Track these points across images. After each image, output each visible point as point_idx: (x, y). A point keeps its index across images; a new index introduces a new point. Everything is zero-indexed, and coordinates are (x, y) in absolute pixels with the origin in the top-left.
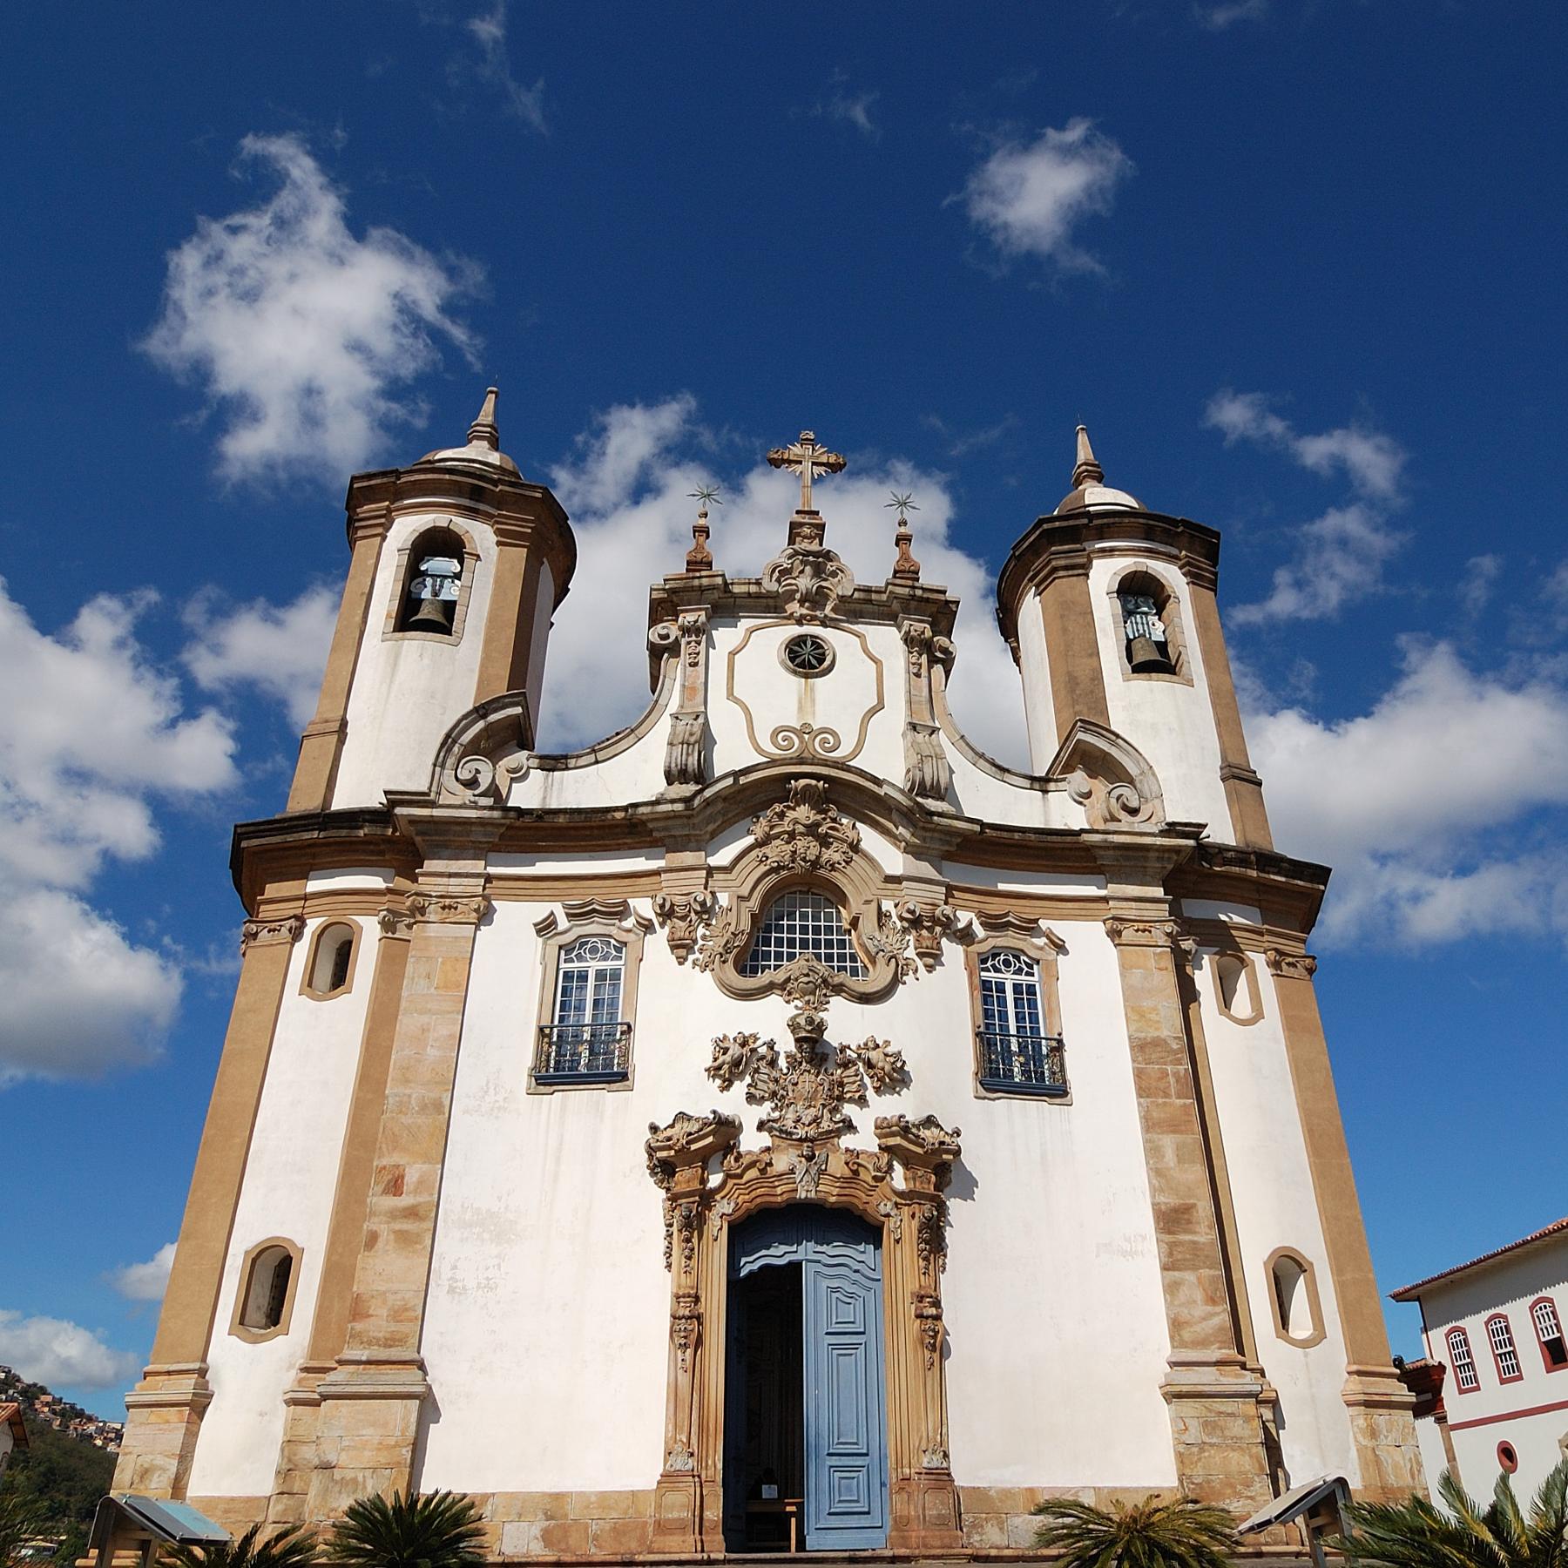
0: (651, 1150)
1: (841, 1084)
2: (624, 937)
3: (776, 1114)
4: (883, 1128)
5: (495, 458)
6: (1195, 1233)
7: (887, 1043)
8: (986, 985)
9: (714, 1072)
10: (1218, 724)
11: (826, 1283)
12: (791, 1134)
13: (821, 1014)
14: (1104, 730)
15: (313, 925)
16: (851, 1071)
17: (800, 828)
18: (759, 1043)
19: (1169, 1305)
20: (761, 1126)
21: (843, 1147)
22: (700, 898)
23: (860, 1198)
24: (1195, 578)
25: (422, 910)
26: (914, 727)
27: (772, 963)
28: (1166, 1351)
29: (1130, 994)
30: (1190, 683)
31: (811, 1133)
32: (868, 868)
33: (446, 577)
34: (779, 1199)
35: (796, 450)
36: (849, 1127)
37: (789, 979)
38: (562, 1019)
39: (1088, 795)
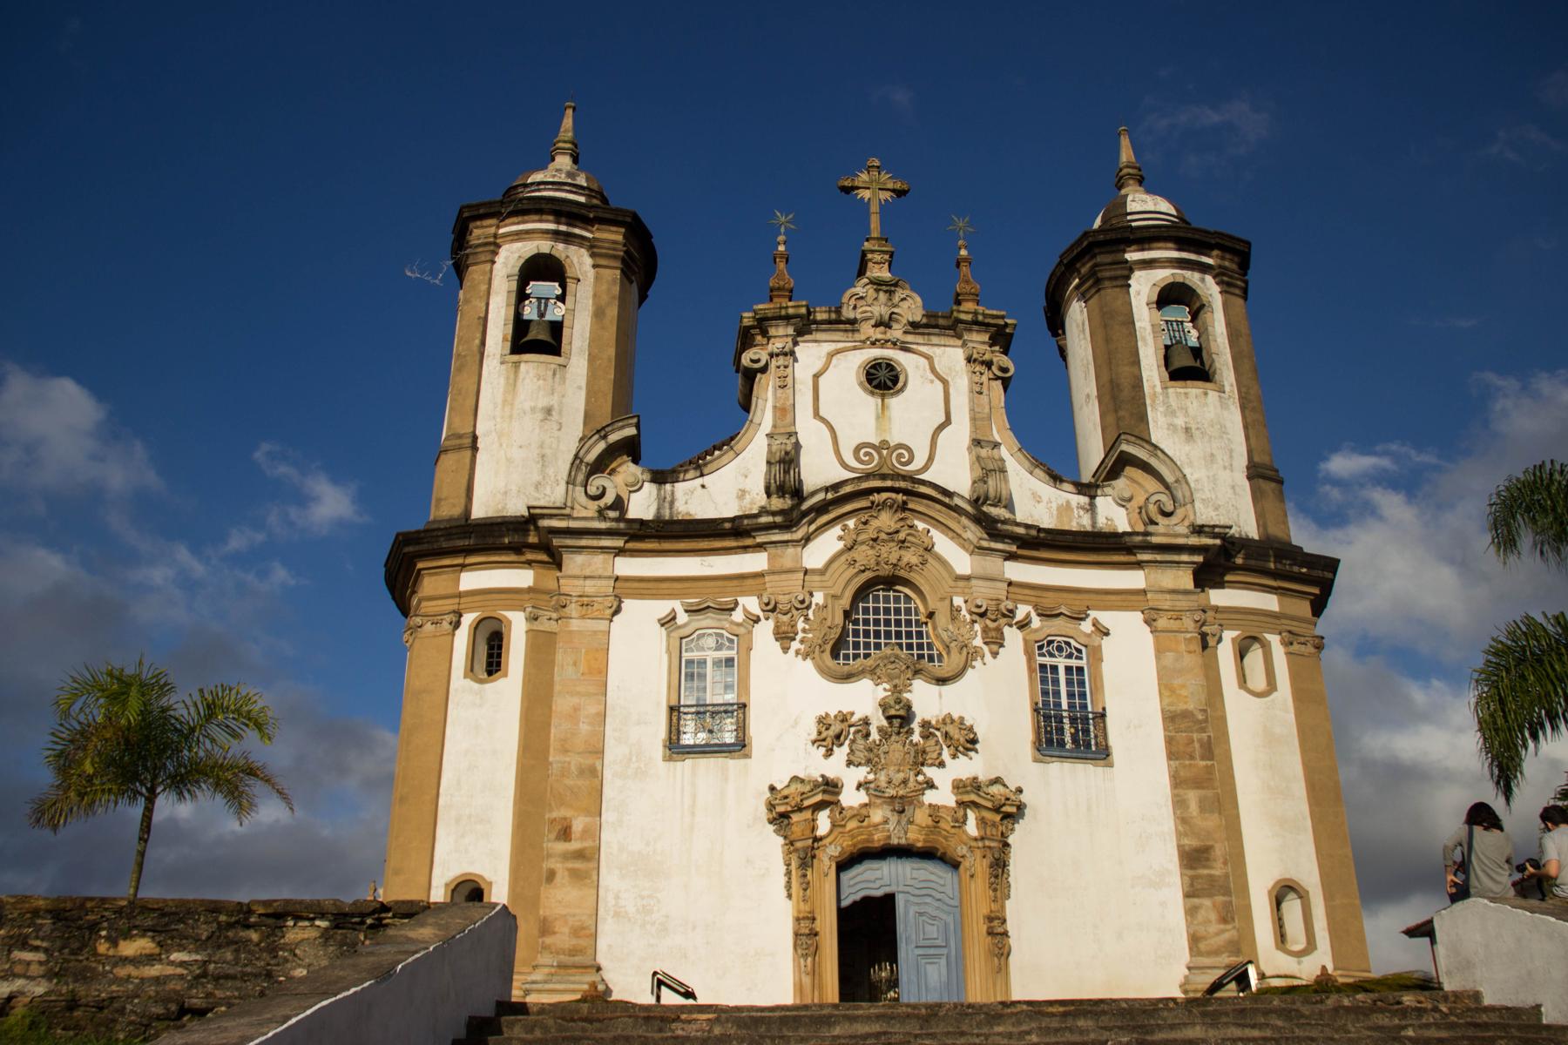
0: (771, 806)
1: (924, 752)
3: (871, 777)
4: (958, 786)
8: (1043, 667)
9: (818, 741)
10: (1246, 427)
11: (917, 908)
15: (468, 619)
16: (932, 742)
17: (883, 536)
23: (941, 844)
24: (1226, 287)
26: (977, 443)
27: (862, 651)
28: (1185, 956)
31: (901, 793)
32: (941, 569)
36: (930, 785)
39: (1130, 500)
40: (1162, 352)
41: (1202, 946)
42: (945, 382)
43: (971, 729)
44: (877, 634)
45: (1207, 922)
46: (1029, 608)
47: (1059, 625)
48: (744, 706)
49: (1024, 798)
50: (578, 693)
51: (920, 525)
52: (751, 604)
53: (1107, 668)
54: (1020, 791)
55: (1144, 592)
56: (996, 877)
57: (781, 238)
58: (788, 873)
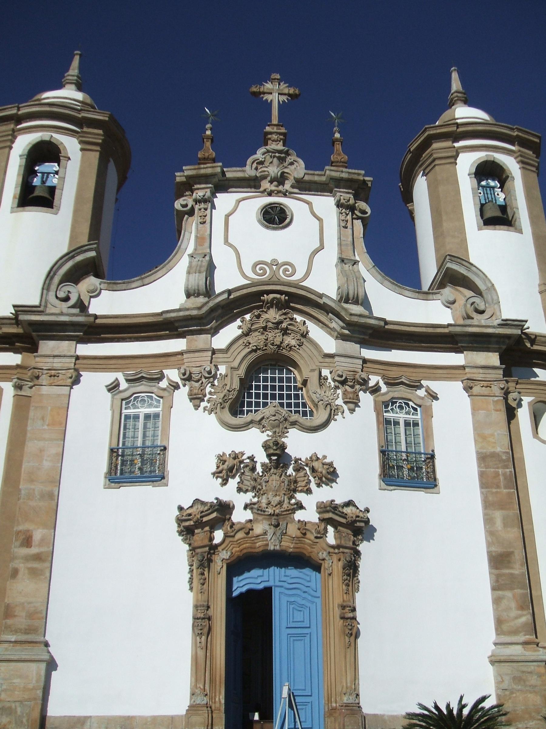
0: (179, 521)
2: (162, 393)
3: (255, 500)
4: (322, 508)
5: (80, 96)
6: (512, 568)
7: (325, 457)
8: (388, 422)
12: (264, 511)
13: (283, 440)
14: (464, 261)
16: (302, 474)
18: (245, 457)
19: (495, 610)
20: (246, 507)
21: (296, 519)
22: (208, 369)
25: (38, 377)
26: (342, 260)
27: (253, 408)
29: (477, 427)
30: (520, 231)
32: (313, 350)
33: (49, 173)
34: (257, 550)
35: (269, 86)
36: (300, 506)
37: (263, 418)
38: (124, 444)
39: (454, 302)
40: (479, 206)
41: (505, 627)
42: (320, 220)
43: (331, 464)
44: (265, 396)
45: (509, 609)
46: (379, 378)
47: (401, 392)
48: (165, 449)
49: (369, 515)
50: (44, 439)
51: (299, 318)
52: (173, 374)
53: (436, 422)
54: (367, 510)
55: (463, 367)
56: (349, 575)
57: (209, 126)
58: (191, 571)
